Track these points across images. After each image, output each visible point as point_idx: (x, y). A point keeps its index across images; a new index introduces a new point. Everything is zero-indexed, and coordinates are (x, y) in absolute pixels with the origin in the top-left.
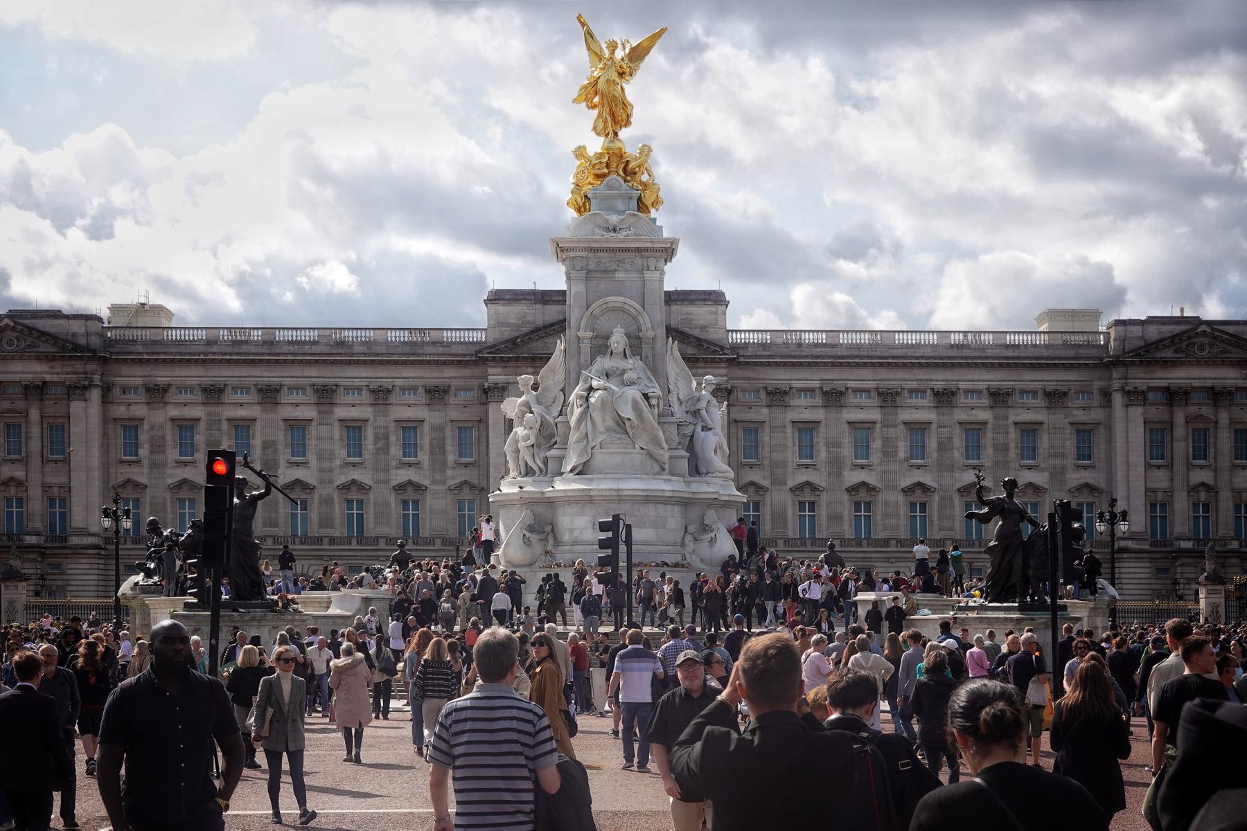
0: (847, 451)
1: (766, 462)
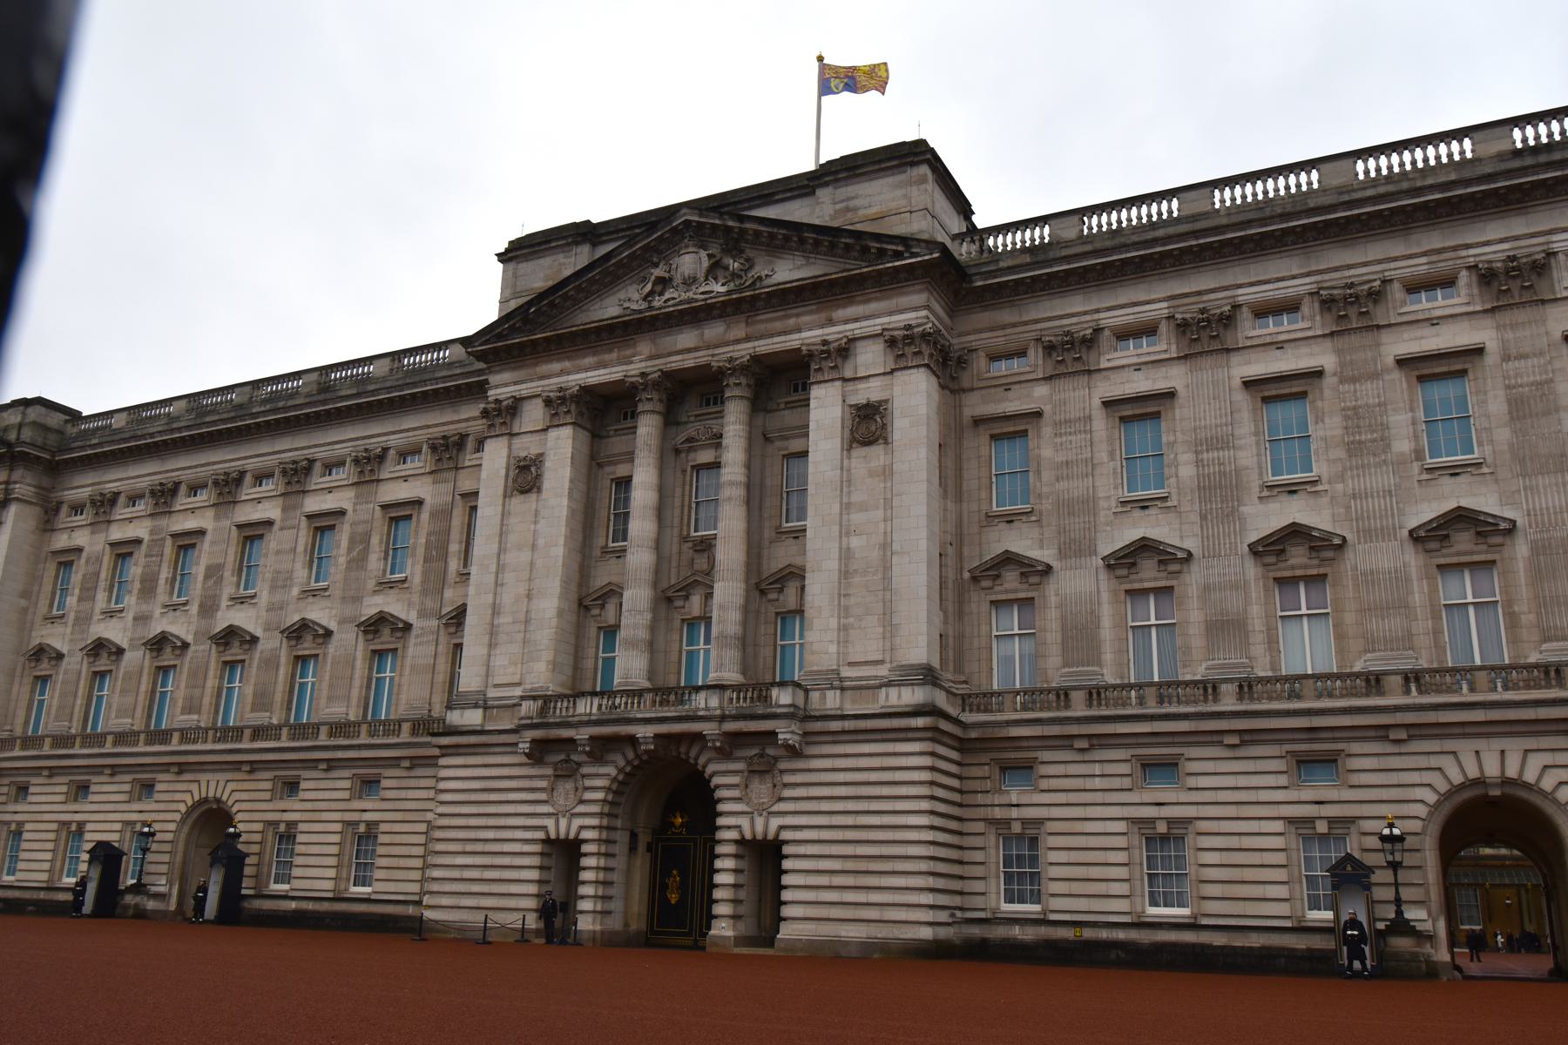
0: (1248, 456)
1: (1046, 505)
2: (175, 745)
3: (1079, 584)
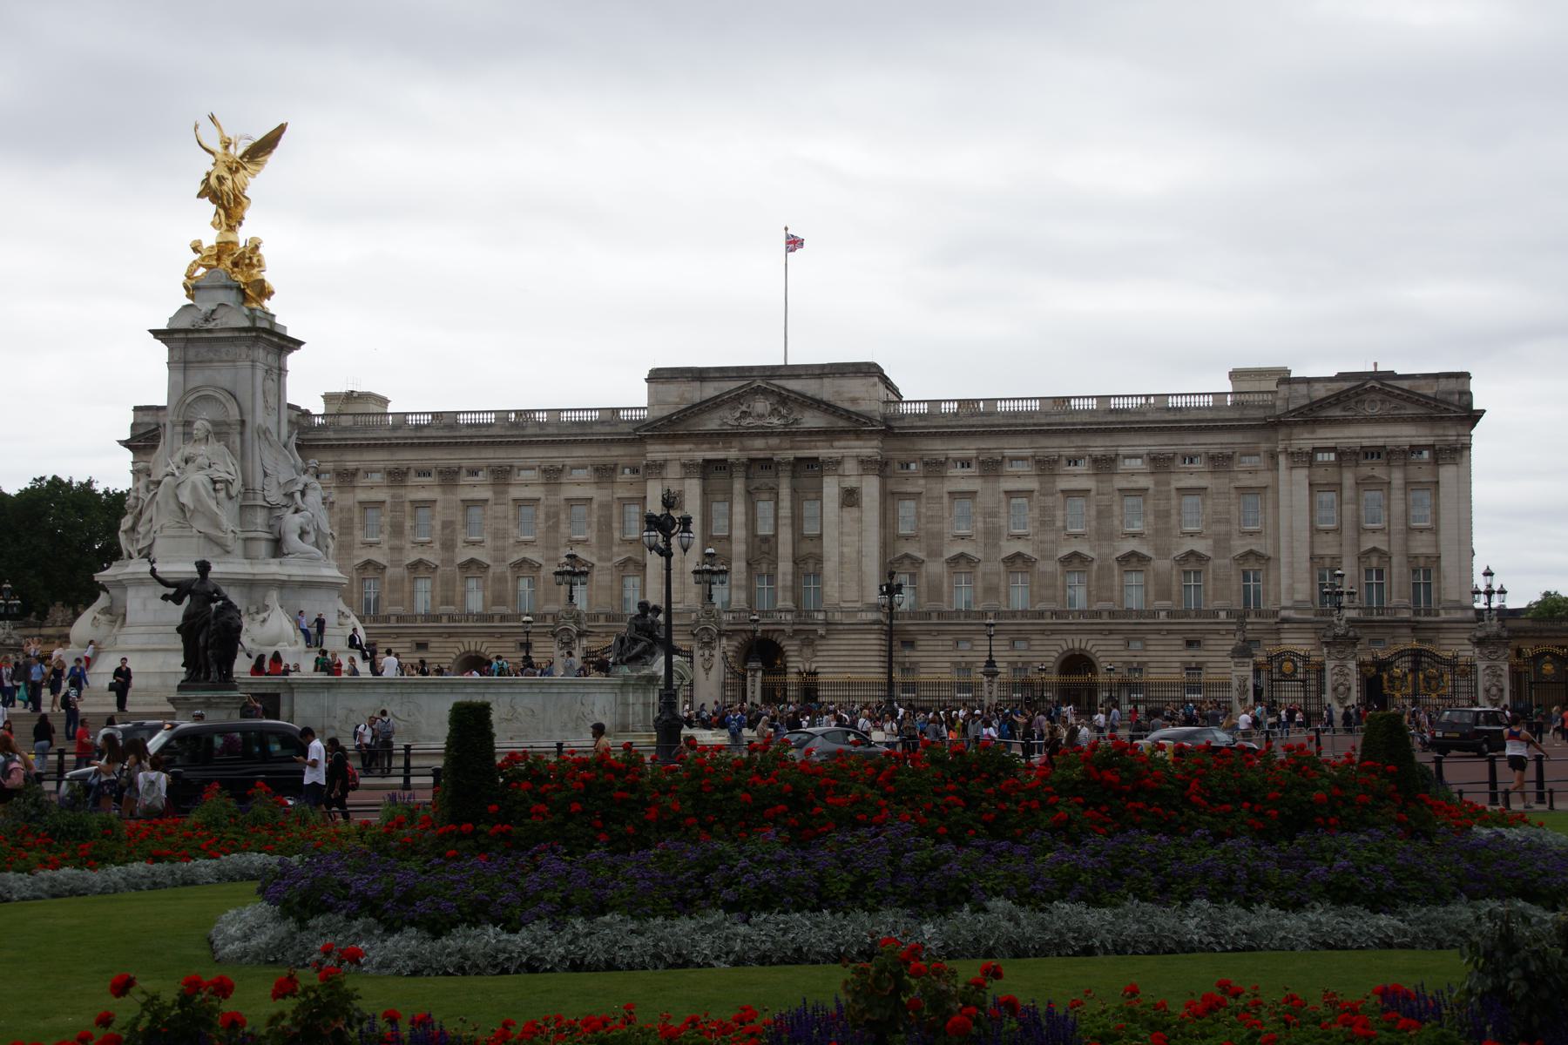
1: (922, 533)
2: (445, 623)
3: (935, 568)
